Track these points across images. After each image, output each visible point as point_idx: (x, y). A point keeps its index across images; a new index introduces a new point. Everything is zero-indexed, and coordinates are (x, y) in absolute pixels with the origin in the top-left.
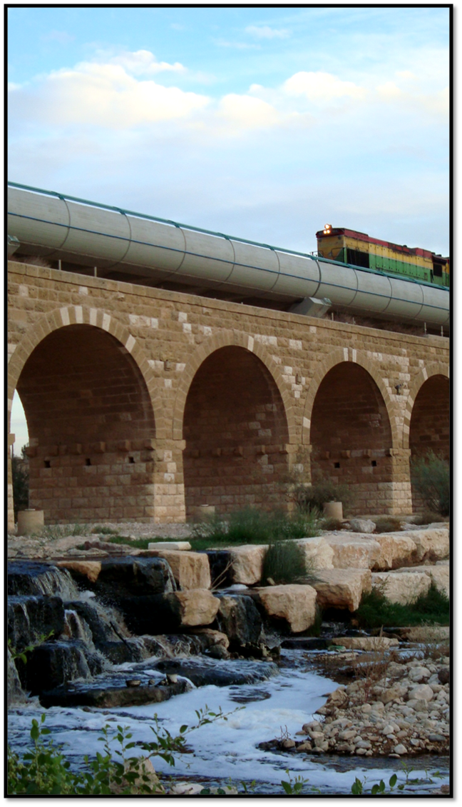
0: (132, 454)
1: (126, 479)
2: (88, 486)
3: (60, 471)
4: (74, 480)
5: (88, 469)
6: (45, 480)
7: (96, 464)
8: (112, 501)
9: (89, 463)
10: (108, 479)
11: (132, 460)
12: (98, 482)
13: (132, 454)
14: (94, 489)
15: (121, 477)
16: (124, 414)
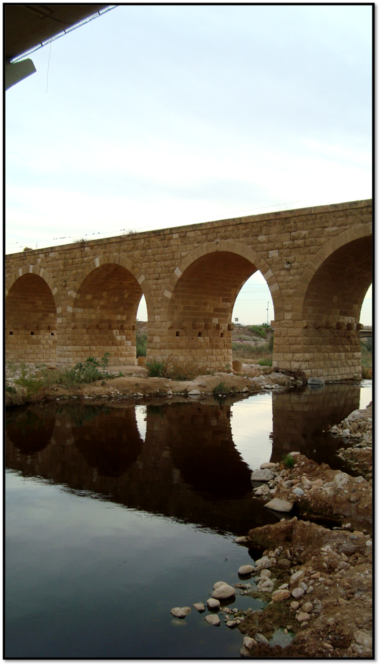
0: (53, 331)
1: (51, 342)
2: (33, 344)
3: (19, 336)
4: (26, 341)
5: (34, 337)
6: (11, 340)
7: (37, 334)
8: (44, 351)
9: (32, 334)
10: (42, 341)
11: (52, 334)
12: (38, 342)
13: (53, 331)
14: (36, 346)
15: (49, 341)
16: (51, 314)
